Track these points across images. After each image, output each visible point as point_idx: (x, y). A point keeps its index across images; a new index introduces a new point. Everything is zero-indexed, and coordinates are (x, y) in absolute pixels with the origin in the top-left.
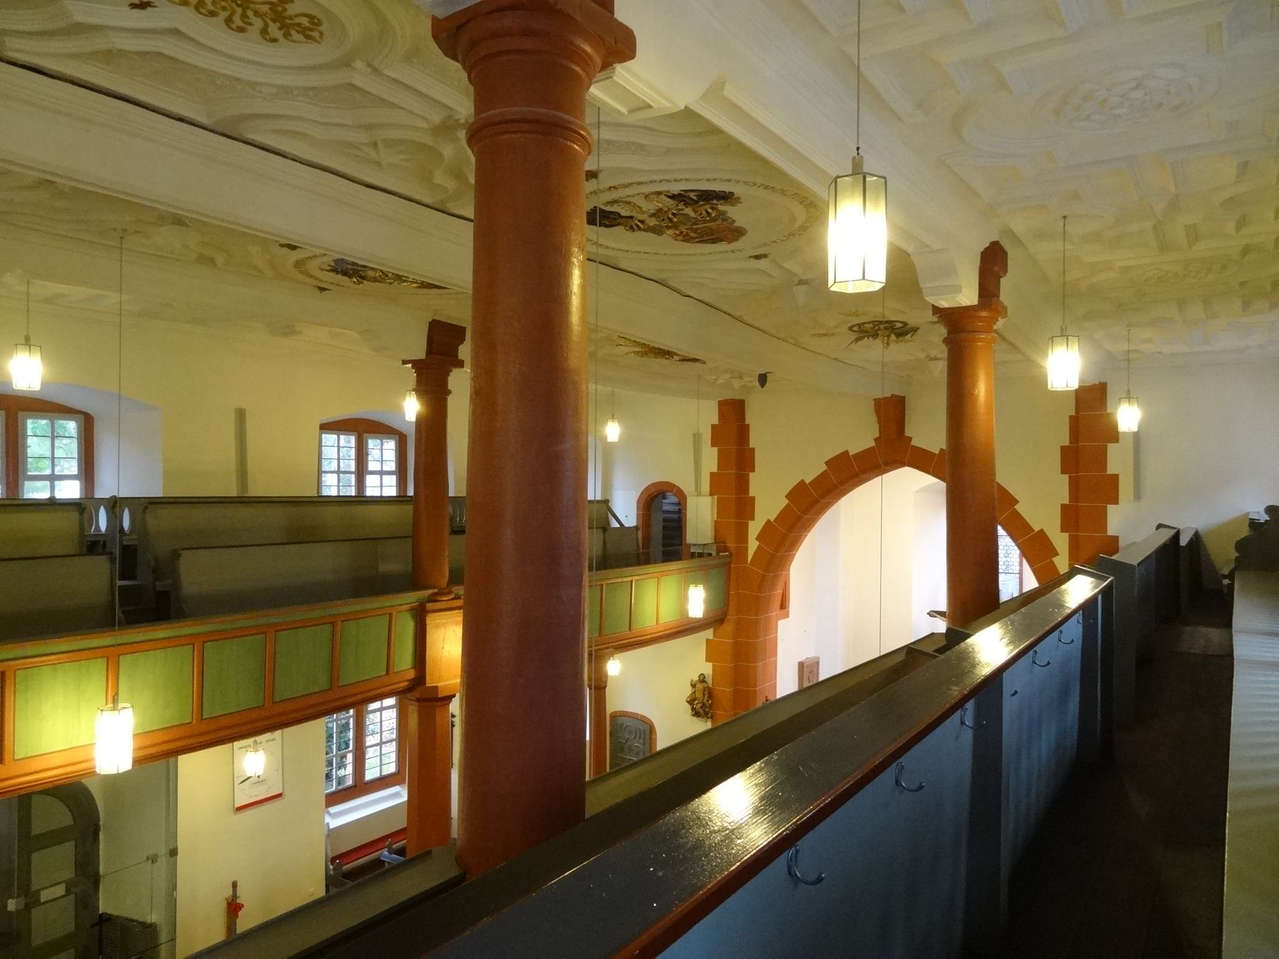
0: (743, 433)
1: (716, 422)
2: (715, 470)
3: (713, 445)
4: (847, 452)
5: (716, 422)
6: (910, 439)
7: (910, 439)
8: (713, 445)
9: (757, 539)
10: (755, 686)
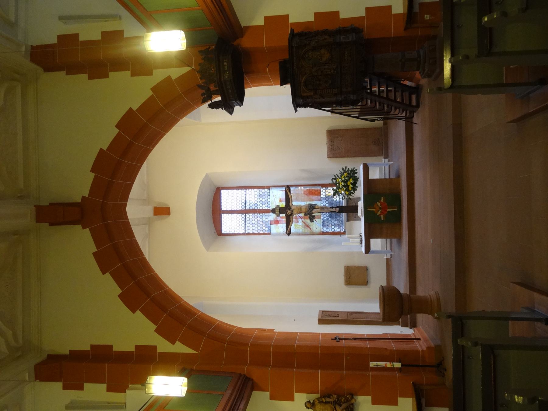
0: (76, 356)
1: (60, 385)
2: (104, 386)
3: (81, 388)
4: (95, 254)
5: (60, 385)
6: (83, 197)
7: (83, 197)
8: (81, 388)
9: (173, 343)
10: (317, 347)
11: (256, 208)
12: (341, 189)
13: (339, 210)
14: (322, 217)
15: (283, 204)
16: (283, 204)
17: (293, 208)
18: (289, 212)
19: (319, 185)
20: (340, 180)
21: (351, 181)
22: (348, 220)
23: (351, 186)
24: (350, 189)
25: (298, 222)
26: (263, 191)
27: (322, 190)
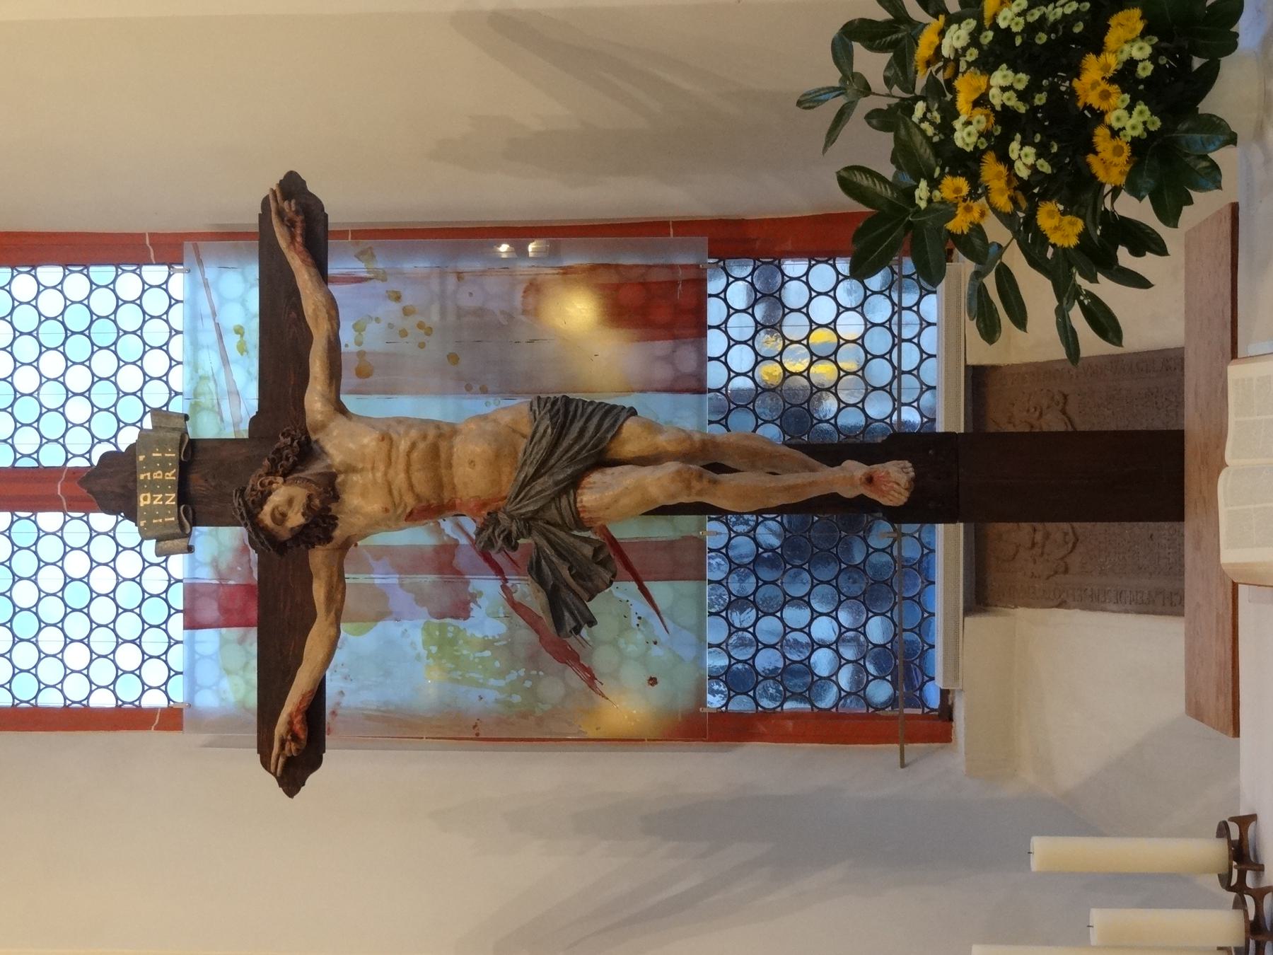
11: (52, 457)
12: (966, 164)
13: (918, 488)
14: (716, 568)
15: (229, 403)
16: (229, 403)
17: (339, 445)
18: (286, 501)
19: (687, 227)
20: (957, 37)
21: (1127, 40)
22: (980, 598)
23: (1130, 119)
24: (1109, 162)
25: (461, 610)
26: (129, 284)
27: (714, 286)
